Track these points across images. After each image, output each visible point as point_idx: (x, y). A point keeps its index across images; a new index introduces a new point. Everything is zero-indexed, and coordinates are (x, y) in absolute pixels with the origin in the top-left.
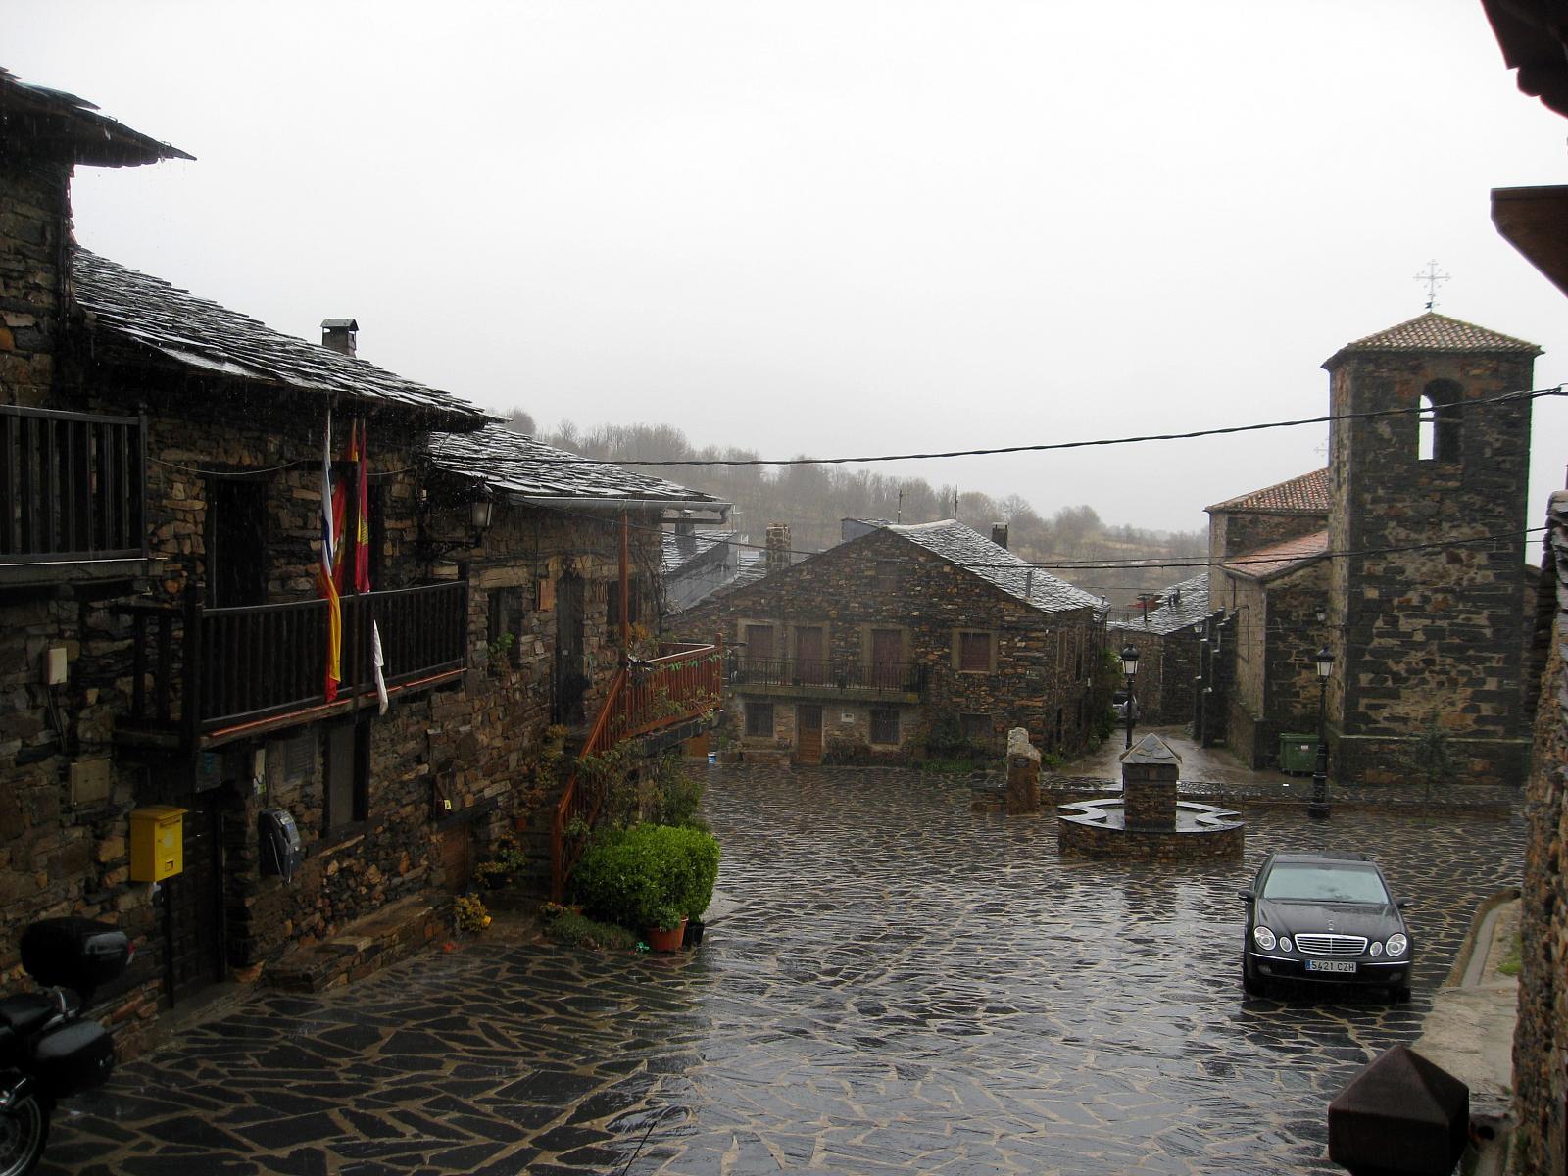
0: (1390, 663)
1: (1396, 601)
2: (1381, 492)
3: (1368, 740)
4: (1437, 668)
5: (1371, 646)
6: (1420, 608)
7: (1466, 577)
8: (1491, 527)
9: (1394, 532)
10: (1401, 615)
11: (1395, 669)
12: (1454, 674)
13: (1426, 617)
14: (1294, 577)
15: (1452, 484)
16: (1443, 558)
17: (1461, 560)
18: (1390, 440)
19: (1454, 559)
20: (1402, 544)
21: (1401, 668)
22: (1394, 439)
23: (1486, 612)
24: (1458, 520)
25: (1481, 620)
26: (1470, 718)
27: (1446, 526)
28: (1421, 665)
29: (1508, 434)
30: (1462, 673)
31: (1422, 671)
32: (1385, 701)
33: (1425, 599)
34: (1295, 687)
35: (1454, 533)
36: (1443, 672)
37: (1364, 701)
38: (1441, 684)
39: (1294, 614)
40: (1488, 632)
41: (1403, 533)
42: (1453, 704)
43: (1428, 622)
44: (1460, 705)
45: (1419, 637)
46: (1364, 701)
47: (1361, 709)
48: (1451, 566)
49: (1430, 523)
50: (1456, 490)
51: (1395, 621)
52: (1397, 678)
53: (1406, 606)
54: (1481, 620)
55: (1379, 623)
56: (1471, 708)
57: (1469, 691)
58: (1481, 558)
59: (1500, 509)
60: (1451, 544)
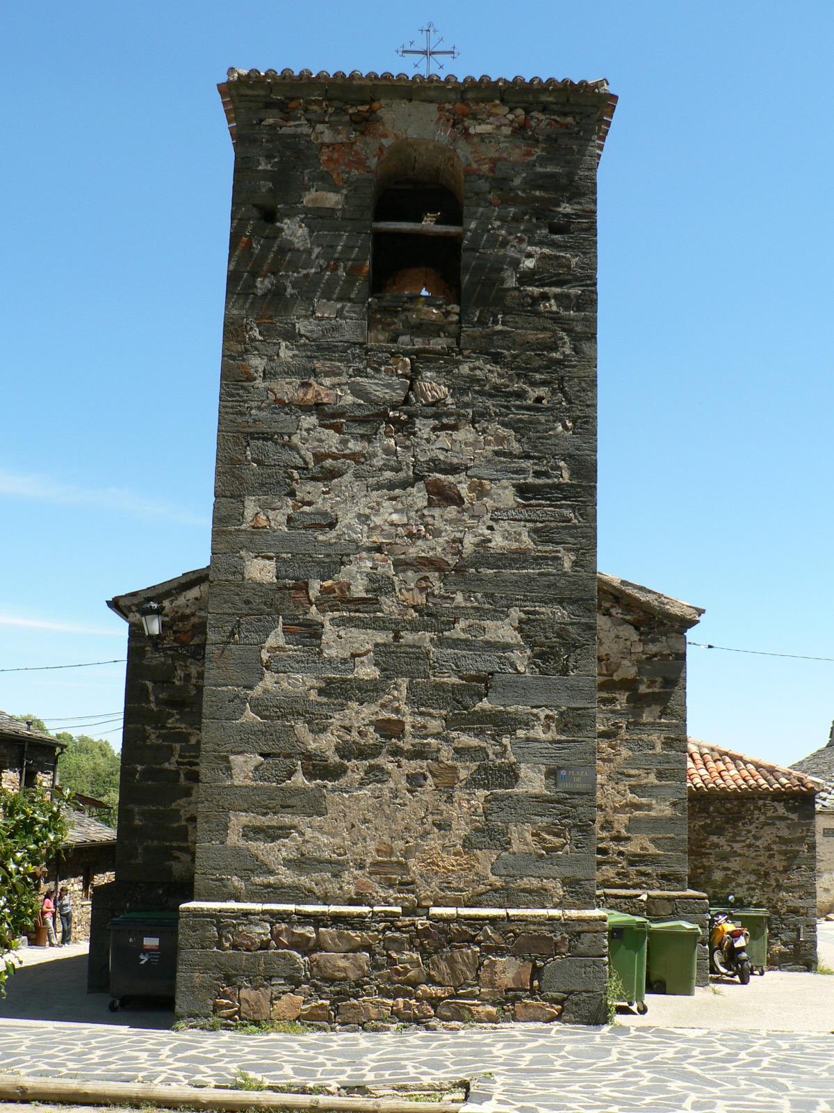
0: (301, 728)
1: (315, 587)
2: (285, 353)
3: (246, 914)
4: (407, 744)
5: (258, 690)
6: (369, 603)
7: (469, 541)
8: (519, 428)
9: (313, 439)
10: (326, 619)
11: (313, 744)
12: (446, 754)
13: (378, 625)
14: (181, 600)
15: (439, 343)
16: (418, 496)
17: (458, 501)
18: (309, 252)
19: (443, 496)
20: (329, 462)
21: (325, 744)
22: (316, 250)
23: (516, 613)
24: (449, 415)
25: (503, 631)
26: (485, 859)
27: (423, 427)
28: (373, 737)
29: (553, 245)
30: (460, 752)
31: (374, 751)
32: (287, 819)
33: (380, 586)
34: (179, 818)
35: (444, 439)
36: (419, 754)
37: (239, 820)
38: (415, 781)
39: (180, 673)
40: (521, 659)
41: (331, 440)
42: (443, 826)
43: (382, 637)
44: (461, 829)
45: (367, 671)
46: (239, 820)
47: (234, 838)
48: (437, 512)
49: (390, 421)
50: (445, 353)
51: (312, 632)
52: (319, 769)
53: (338, 599)
54: (503, 631)
55: (276, 638)
56: (488, 834)
57: (482, 793)
58: (506, 496)
59: (542, 391)
60: (436, 466)
